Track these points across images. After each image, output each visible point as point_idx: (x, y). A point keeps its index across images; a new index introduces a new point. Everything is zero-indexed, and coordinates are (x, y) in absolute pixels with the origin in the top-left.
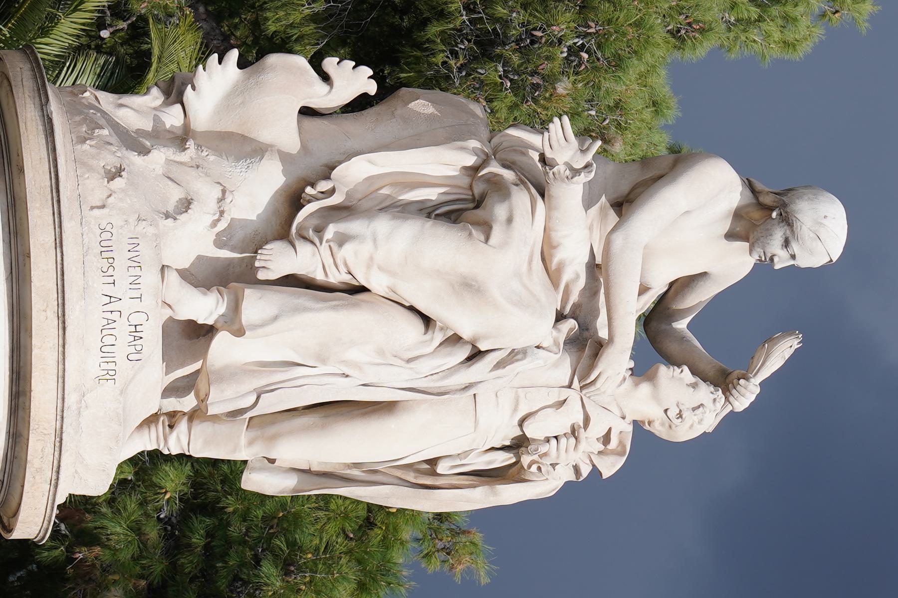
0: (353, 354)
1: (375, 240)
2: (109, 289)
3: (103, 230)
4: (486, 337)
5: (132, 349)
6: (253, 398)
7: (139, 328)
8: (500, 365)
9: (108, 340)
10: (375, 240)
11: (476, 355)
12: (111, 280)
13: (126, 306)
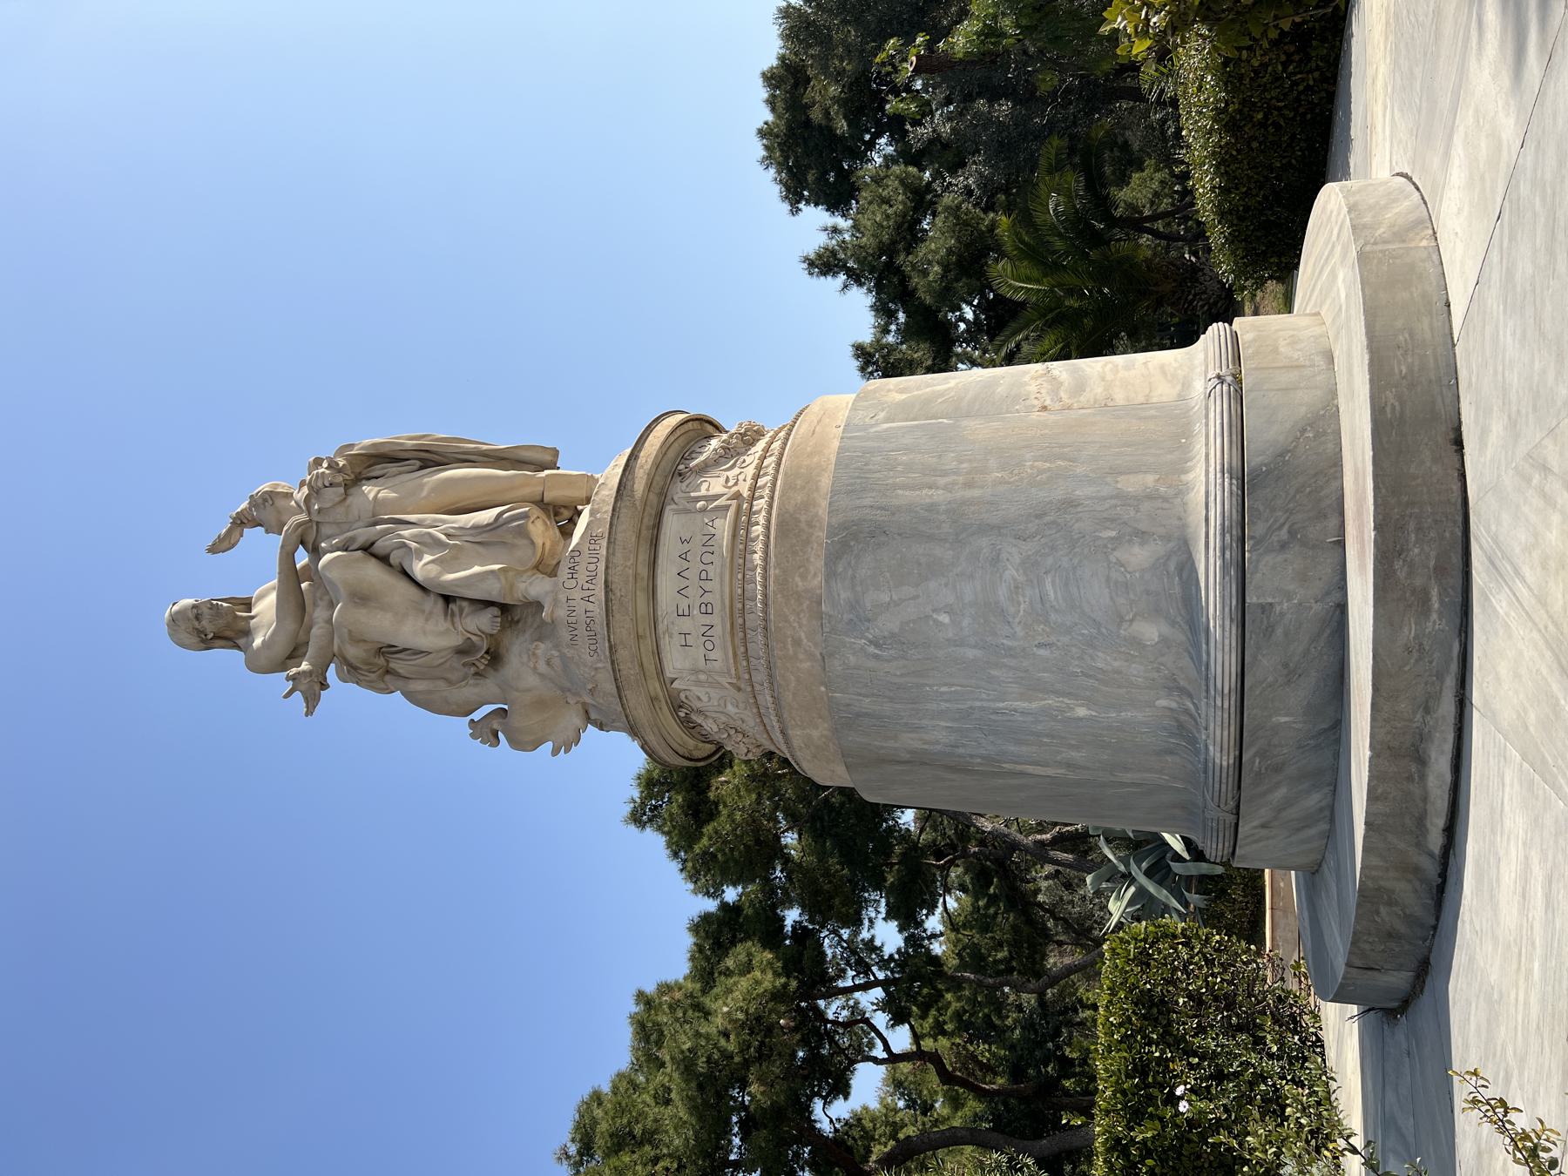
2: (590, 607)
3: (595, 651)
5: (577, 559)
7: (570, 576)
8: (353, 539)
9: (592, 567)
12: (588, 614)
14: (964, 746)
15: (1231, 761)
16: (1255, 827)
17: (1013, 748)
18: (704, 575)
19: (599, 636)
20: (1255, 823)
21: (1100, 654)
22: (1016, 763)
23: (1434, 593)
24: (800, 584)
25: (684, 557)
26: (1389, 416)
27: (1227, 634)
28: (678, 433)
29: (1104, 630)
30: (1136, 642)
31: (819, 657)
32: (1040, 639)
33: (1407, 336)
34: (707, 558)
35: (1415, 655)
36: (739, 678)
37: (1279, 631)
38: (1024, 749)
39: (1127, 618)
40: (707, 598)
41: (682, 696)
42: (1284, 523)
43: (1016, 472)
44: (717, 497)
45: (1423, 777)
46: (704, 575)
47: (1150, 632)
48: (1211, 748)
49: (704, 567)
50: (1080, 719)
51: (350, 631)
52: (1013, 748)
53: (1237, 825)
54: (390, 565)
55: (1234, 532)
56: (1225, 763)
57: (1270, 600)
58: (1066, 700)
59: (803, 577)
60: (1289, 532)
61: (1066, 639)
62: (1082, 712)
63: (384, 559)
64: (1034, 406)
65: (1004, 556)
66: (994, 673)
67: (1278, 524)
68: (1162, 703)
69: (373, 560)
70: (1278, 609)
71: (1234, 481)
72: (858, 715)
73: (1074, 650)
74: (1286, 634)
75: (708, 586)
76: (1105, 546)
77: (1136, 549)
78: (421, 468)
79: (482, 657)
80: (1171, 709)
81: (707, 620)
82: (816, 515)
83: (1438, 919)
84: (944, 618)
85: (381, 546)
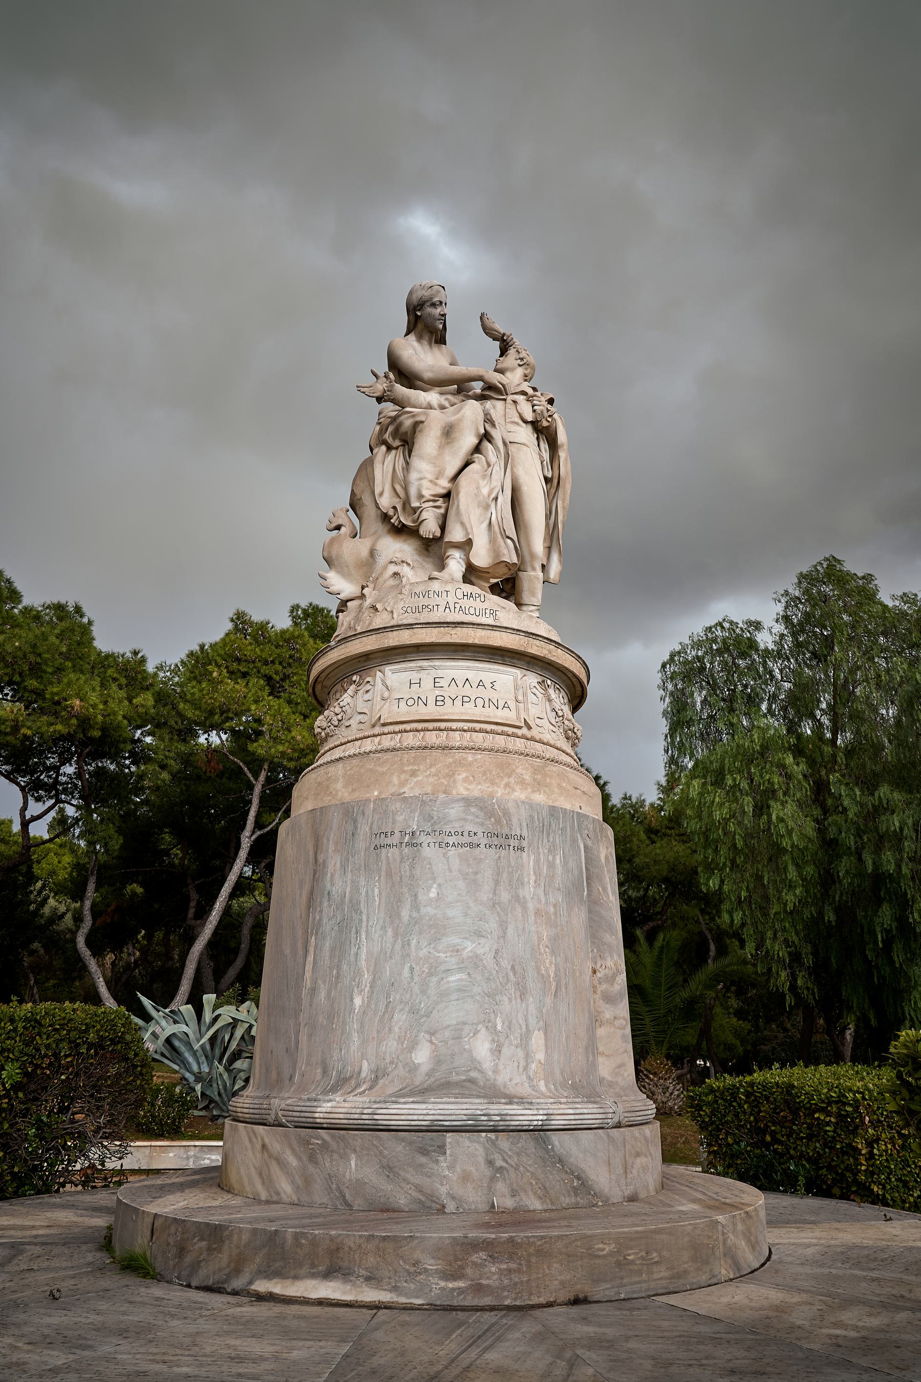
0: (485, 491)
1: (421, 479)
2: (441, 609)
3: (406, 611)
4: (477, 429)
6: (509, 541)
8: (493, 425)
10: (421, 479)
11: (486, 437)
12: (436, 607)
13: (451, 599)
14: (330, 906)
15: (318, 1120)
16: (263, 1139)
17: (327, 945)
18: (466, 699)
19: (418, 615)
20: (267, 1141)
21: (404, 1017)
22: (316, 947)
23: (461, 1284)
24: (461, 777)
25: (481, 684)
26: (596, 1247)
27: (421, 1118)
28: (574, 680)
29: (423, 1020)
30: (414, 1045)
31: (402, 791)
32: (417, 969)
33: (656, 1259)
34: (480, 702)
35: (412, 1269)
36: (384, 725)
37: (423, 1160)
38: (327, 954)
39: (433, 1038)
40: (448, 702)
41: (368, 679)
42: (507, 1162)
43: (547, 950)
44: (526, 710)
45: (313, 1276)
46: (466, 699)
47: (422, 1056)
48: (329, 1104)
49: (473, 699)
50: (352, 999)
51: (422, 422)
52: (328, 945)
53: (265, 1124)
54: (472, 454)
55: (501, 1123)
56: (317, 1115)
57: (448, 1152)
58: (367, 989)
59: (465, 780)
60: (501, 1167)
61: (416, 989)
62: (358, 1001)
63: (477, 449)
64: (596, 963)
65: (483, 941)
66: (390, 932)
67: (507, 1158)
68: (365, 1065)
69: (477, 441)
70: (441, 1158)
71: (540, 1123)
72: (355, 821)
73: (408, 996)
74: (421, 1165)
75: (458, 702)
76: (489, 1021)
77: (487, 1045)
78: (546, 479)
79: (400, 521)
80: (360, 1072)
81: (431, 701)
82: (514, 790)
83: (197, 1288)
84: (433, 894)
85: (486, 444)
